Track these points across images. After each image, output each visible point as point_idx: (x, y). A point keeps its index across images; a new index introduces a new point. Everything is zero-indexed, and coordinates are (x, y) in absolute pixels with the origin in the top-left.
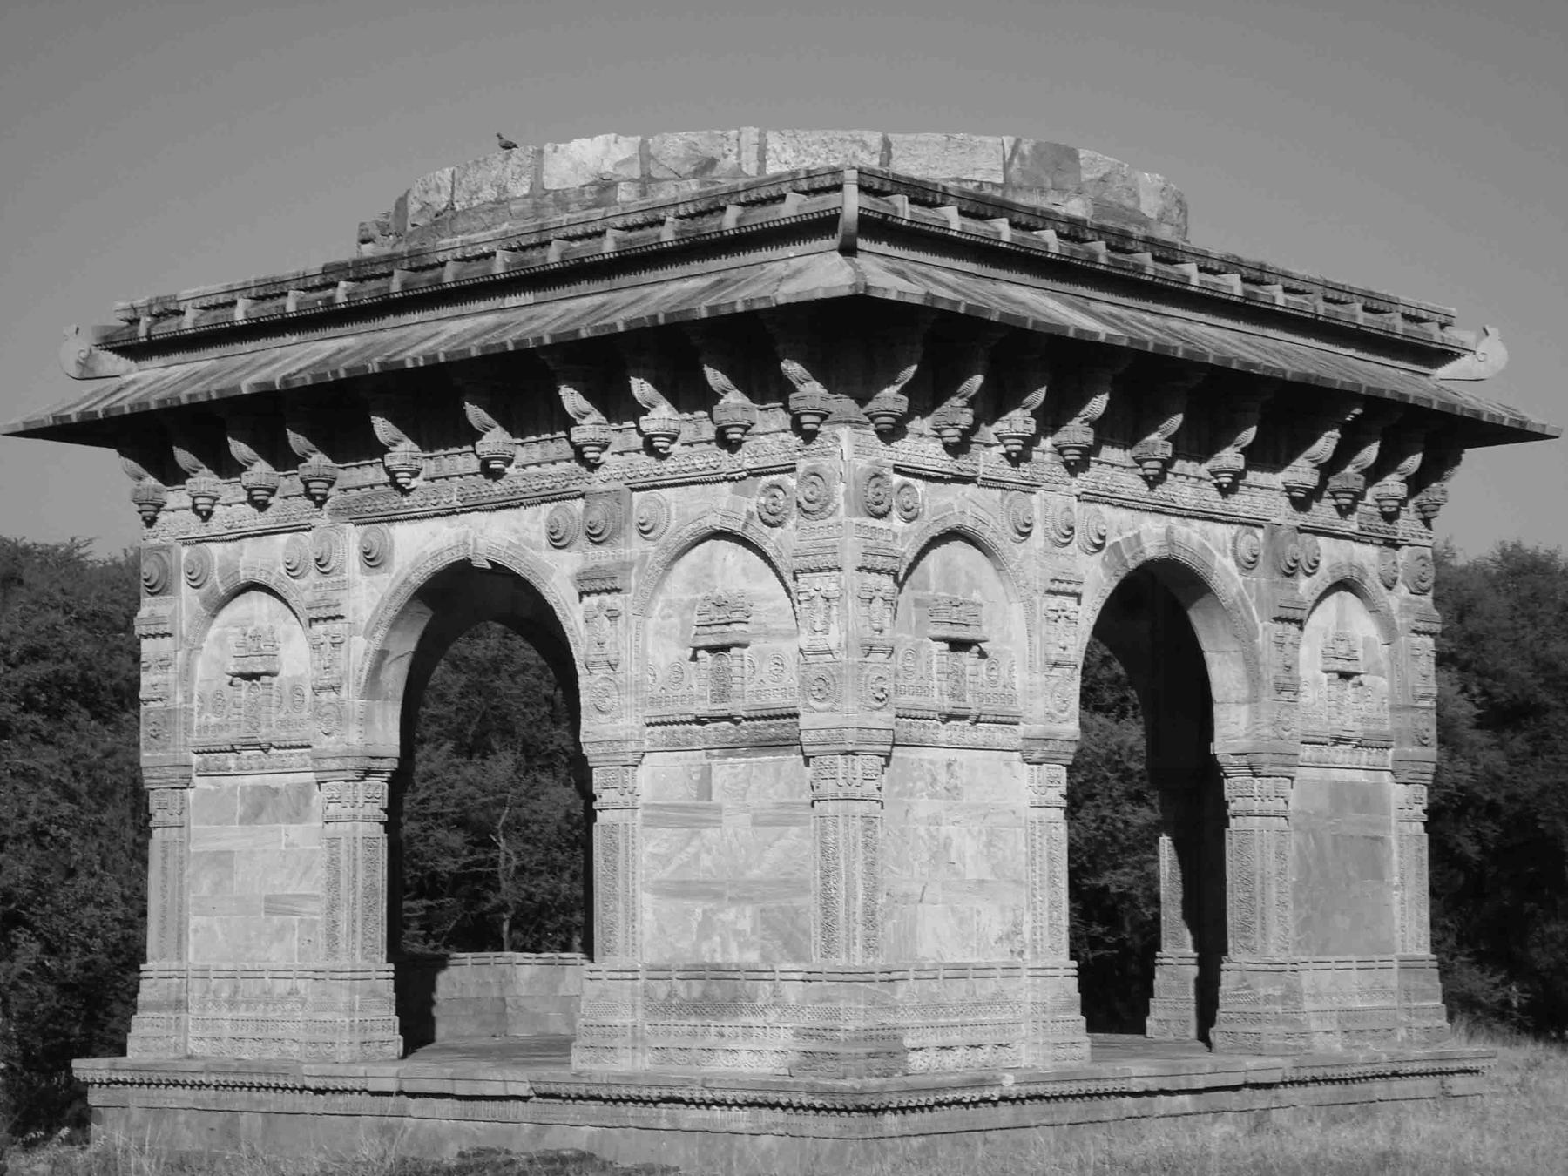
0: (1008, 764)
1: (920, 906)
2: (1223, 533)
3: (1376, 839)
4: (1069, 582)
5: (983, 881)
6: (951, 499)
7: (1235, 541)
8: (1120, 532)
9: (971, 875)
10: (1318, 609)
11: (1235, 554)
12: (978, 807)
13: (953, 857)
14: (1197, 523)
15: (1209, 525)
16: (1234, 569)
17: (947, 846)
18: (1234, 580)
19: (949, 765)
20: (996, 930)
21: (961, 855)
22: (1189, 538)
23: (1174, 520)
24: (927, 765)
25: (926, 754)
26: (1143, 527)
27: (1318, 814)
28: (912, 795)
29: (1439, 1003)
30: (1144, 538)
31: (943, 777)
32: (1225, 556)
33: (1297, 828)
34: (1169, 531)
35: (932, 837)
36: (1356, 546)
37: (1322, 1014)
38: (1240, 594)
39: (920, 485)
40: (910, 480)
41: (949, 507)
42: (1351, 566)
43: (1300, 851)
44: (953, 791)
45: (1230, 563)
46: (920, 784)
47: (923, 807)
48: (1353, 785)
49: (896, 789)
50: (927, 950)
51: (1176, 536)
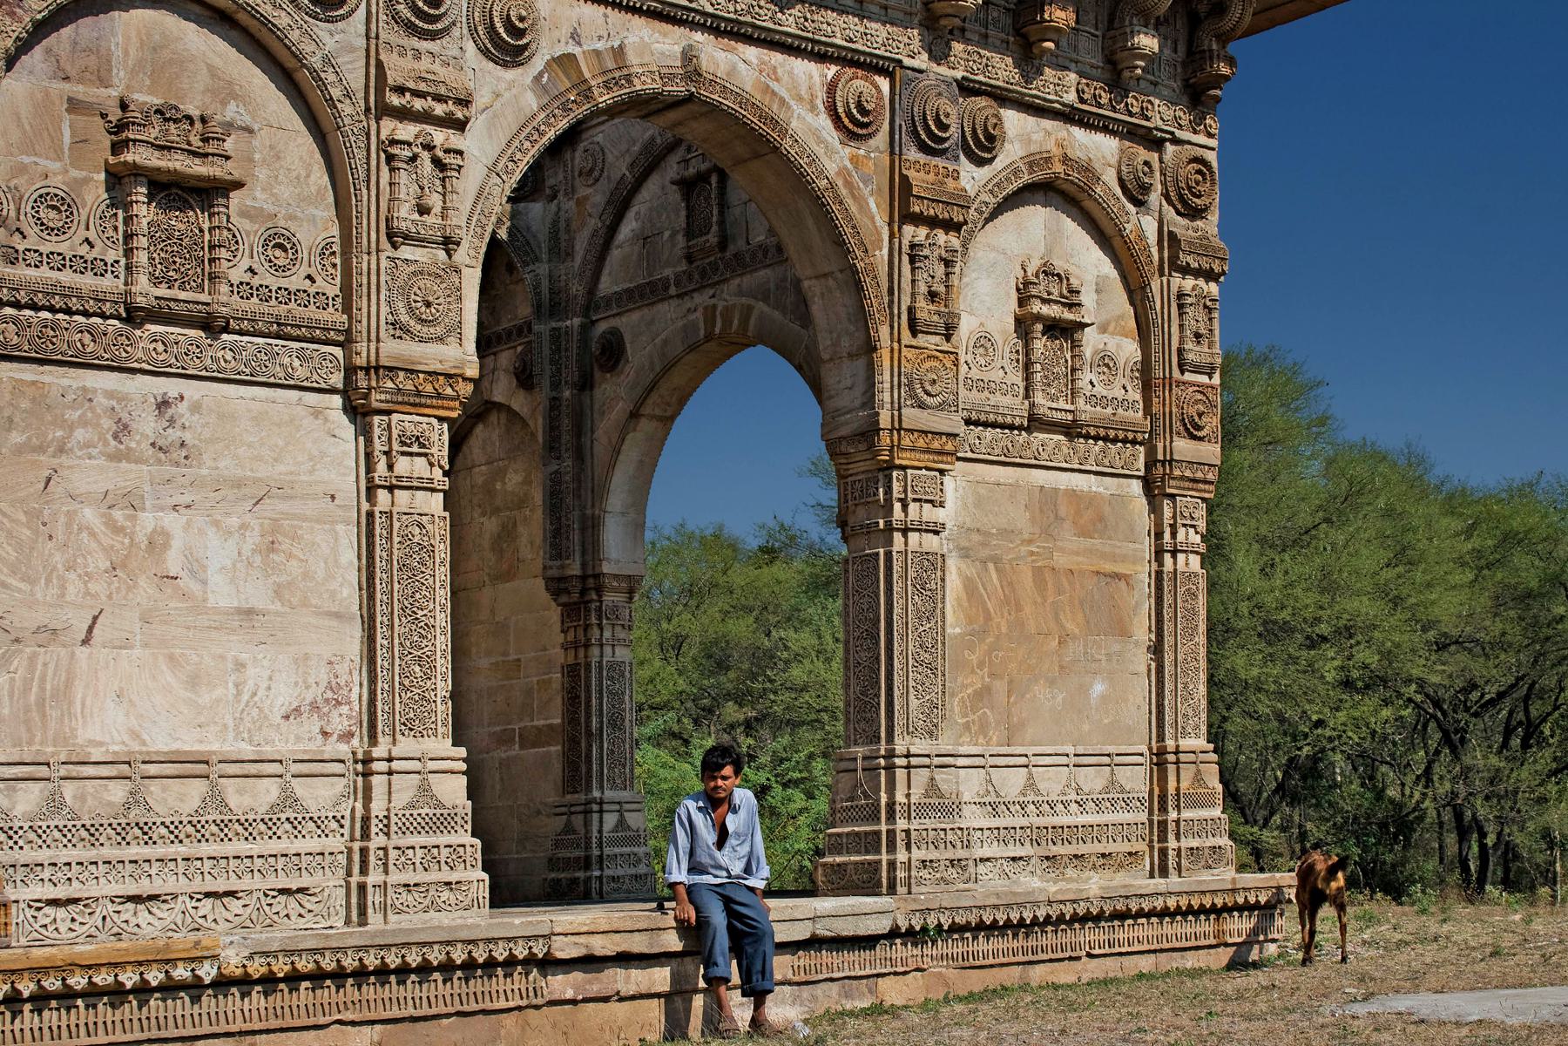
0: (317, 413)
1: (82, 653)
2: (809, 74)
3: (1117, 576)
4: (439, 98)
5: (249, 612)
7: (832, 88)
8: (575, 37)
9: (222, 595)
10: (1008, 218)
11: (832, 110)
12: (238, 484)
13: (173, 564)
14: (752, 53)
15: (777, 58)
17: (157, 543)
18: (830, 151)
20: (284, 696)
21: (196, 568)
22: (733, 70)
23: (698, 36)
24: (101, 401)
26: (631, 40)
27: (1005, 533)
28: (61, 450)
29: (1217, 812)
30: (632, 58)
31: (147, 425)
32: (813, 108)
33: (965, 553)
34: (688, 56)
35: (118, 530)
36: (1078, 133)
37: (1003, 835)
38: (842, 172)
42: (1066, 159)
43: (969, 586)
44: (183, 452)
45: (824, 122)
46: (80, 434)
47: (90, 474)
48: (1072, 494)
50: (104, 728)
51: (705, 65)
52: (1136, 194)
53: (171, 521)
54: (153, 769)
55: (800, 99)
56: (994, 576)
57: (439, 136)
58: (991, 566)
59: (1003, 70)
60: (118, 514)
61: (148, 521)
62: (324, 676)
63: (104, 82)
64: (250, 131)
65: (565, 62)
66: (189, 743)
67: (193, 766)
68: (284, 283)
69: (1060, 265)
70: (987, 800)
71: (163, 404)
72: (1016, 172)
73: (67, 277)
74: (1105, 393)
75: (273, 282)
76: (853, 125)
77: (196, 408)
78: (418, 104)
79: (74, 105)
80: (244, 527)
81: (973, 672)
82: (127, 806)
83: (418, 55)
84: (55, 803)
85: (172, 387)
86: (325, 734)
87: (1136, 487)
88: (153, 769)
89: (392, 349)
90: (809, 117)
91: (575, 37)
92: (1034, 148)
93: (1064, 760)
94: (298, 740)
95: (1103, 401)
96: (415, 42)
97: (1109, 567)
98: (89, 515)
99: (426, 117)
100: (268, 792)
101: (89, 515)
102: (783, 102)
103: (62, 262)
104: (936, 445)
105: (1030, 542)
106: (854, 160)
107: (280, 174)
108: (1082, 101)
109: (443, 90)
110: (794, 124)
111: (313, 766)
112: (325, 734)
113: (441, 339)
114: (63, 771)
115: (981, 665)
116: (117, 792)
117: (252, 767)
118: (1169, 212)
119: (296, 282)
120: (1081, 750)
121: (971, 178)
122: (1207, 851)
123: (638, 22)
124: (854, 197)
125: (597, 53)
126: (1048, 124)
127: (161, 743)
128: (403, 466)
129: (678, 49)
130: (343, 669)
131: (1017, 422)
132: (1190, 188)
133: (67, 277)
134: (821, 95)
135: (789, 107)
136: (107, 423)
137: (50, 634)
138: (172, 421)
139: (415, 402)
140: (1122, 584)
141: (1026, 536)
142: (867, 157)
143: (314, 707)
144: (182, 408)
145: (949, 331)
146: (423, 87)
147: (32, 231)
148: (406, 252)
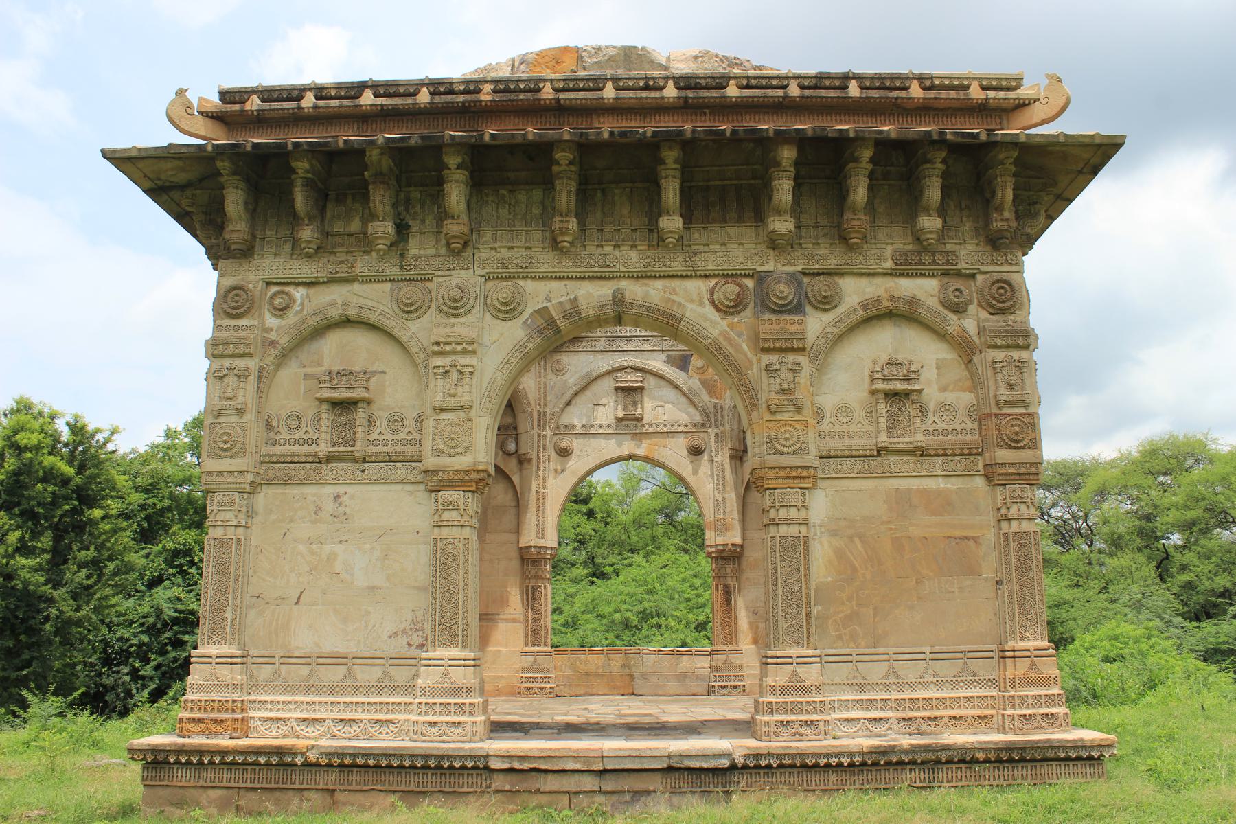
0: (411, 494)
5: (373, 588)
6: (333, 297)
8: (548, 299)
11: (713, 302)
14: (659, 284)
15: (676, 283)
16: (715, 316)
17: (331, 558)
19: (338, 496)
20: (389, 628)
23: (624, 283)
25: (309, 490)
28: (291, 521)
30: (582, 301)
31: (329, 506)
32: (701, 304)
35: (313, 553)
39: (298, 293)
40: (287, 289)
41: (333, 303)
42: (893, 298)
45: (709, 310)
49: (273, 517)
52: (958, 309)
53: (338, 548)
54: (321, 661)
55: (692, 301)
56: (859, 545)
57: (463, 360)
58: (857, 540)
59: (830, 258)
60: (314, 546)
61: (327, 548)
62: (410, 617)
63: (320, 365)
64: (384, 373)
65: (543, 312)
66: (340, 649)
67: (338, 659)
68: (395, 437)
69: (900, 357)
70: (854, 682)
71: (337, 497)
72: (854, 311)
73: (296, 448)
74: (946, 427)
75: (390, 437)
76: (729, 309)
77: (352, 497)
78: (448, 348)
79: (306, 377)
80: (372, 548)
81: (843, 603)
82: (310, 677)
83: (453, 325)
84: (276, 674)
85: (341, 489)
86: (409, 645)
87: (980, 482)
88: (321, 661)
89: (444, 461)
90: (699, 309)
91: (548, 299)
92: (867, 297)
93: (921, 656)
94: (398, 646)
95: (945, 433)
96: (452, 320)
97: (958, 533)
98: (301, 548)
99: (454, 352)
100: (377, 672)
101: (301, 548)
102: (680, 304)
103: (294, 442)
104: (794, 474)
105: (889, 522)
106: (731, 326)
107: (395, 390)
108: (897, 264)
109: (459, 339)
110: (688, 314)
111: (399, 661)
112: (409, 645)
113: (461, 454)
114: (282, 660)
115: (850, 599)
116: (305, 671)
117: (369, 660)
118: (984, 315)
119: (402, 435)
120: (937, 649)
121: (815, 324)
122: (1039, 718)
123: (586, 283)
124: (731, 344)
125: (561, 303)
126: (878, 281)
127: (328, 648)
128: (446, 516)
129: (610, 292)
130: (420, 614)
131: (868, 453)
132: (994, 299)
133: (296, 448)
134: (706, 296)
135: (684, 306)
136: (312, 508)
137: (280, 599)
138: (340, 504)
139: (451, 485)
140: (971, 543)
141: (885, 519)
142: (740, 322)
143: (404, 632)
144: (346, 497)
145: (798, 408)
146: (449, 340)
147: (284, 431)
148: (444, 416)
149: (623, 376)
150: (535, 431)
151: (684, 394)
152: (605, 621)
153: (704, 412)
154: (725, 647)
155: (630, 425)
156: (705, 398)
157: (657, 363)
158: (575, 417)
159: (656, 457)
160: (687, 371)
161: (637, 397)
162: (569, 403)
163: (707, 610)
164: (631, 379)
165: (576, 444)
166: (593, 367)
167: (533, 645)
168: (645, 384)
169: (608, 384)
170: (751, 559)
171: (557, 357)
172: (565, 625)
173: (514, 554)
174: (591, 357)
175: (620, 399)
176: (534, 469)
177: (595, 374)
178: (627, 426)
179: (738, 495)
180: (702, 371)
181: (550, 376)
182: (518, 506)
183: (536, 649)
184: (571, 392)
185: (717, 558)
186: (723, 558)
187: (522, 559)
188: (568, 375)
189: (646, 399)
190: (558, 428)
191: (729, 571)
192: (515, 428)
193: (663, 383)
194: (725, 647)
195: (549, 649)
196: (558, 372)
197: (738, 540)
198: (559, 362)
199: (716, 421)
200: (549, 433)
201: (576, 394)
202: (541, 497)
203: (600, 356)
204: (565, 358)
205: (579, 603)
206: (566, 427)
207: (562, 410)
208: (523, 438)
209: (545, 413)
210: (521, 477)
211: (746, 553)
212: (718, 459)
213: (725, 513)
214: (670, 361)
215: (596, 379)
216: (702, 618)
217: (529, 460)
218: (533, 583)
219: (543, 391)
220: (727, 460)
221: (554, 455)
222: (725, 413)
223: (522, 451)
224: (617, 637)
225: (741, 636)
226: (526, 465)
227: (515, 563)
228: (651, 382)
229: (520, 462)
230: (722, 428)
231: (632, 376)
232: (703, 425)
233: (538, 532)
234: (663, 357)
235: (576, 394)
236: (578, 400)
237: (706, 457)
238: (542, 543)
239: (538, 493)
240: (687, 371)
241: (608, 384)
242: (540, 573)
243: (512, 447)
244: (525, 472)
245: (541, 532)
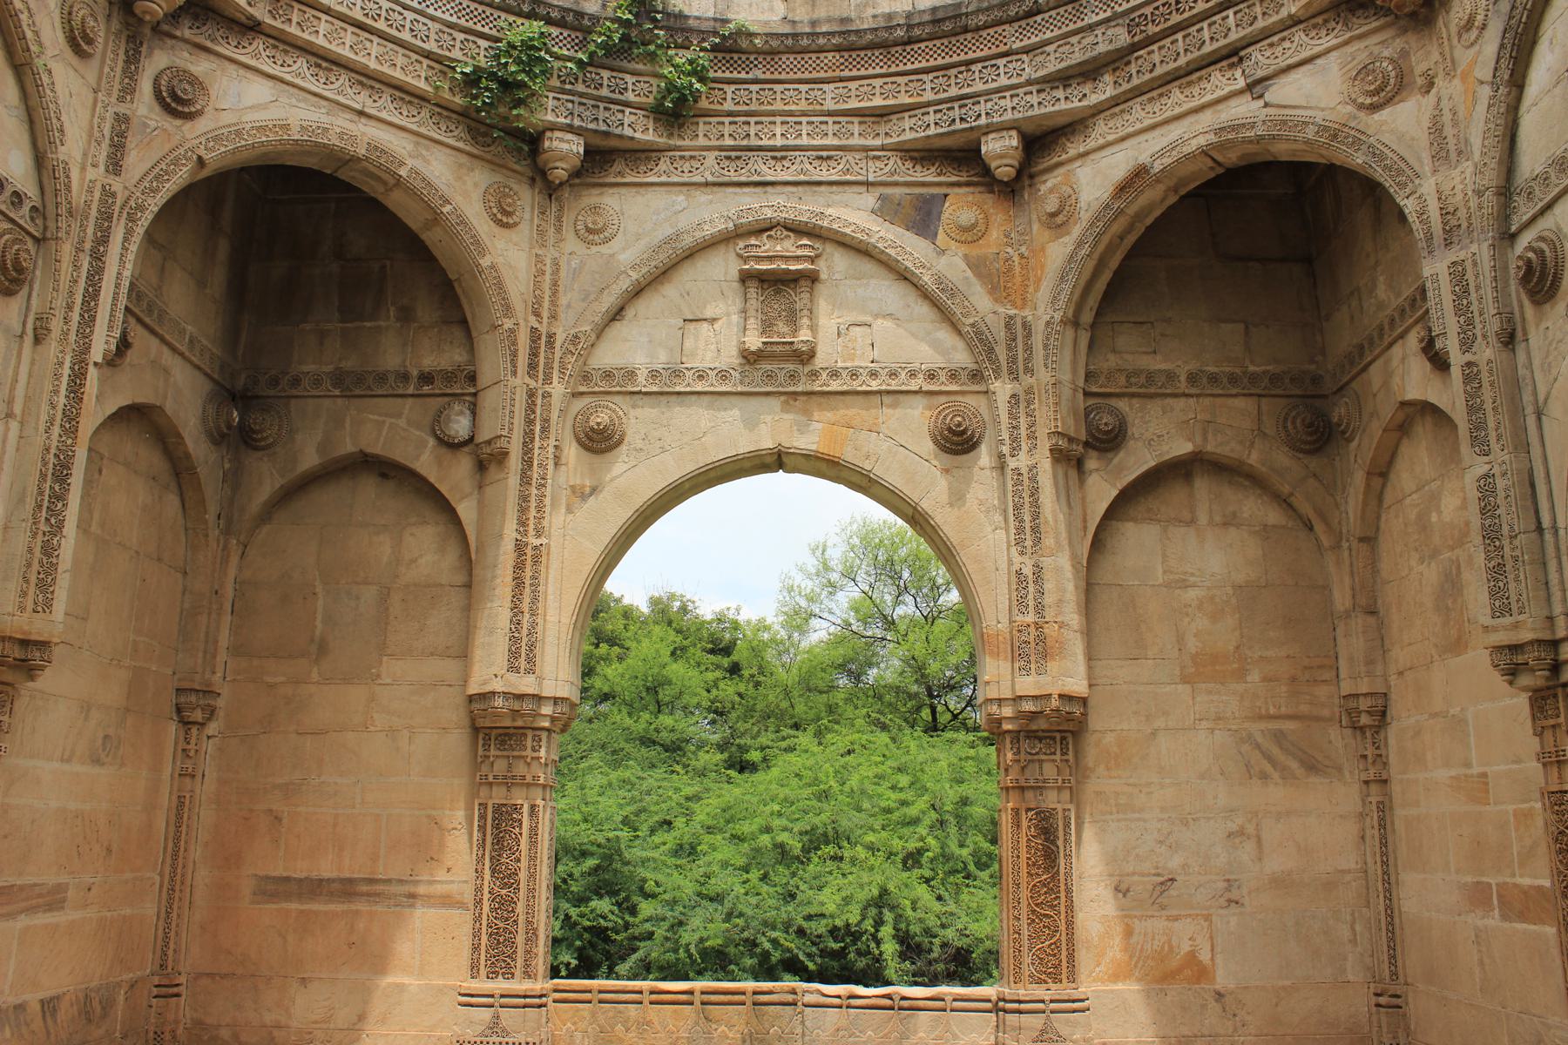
149: (766, 246)
150: (521, 381)
151: (925, 295)
152: (745, 847)
153: (979, 341)
154: (1039, 992)
155: (780, 369)
156: (981, 303)
157: (853, 213)
158: (636, 347)
159: (849, 455)
160: (932, 237)
161: (801, 299)
162: (617, 314)
163: (922, 830)
164: (784, 252)
165: (638, 421)
166: (684, 222)
167: (492, 975)
168: (821, 266)
169: (723, 267)
170: (1109, 739)
171: (591, 198)
172: (678, 851)
173: (454, 715)
174: (680, 199)
175: (754, 303)
176: (513, 481)
177: (688, 241)
178: (770, 376)
179: (1074, 557)
180: (970, 234)
181: (571, 244)
182: (468, 586)
183: (500, 985)
184: (625, 284)
185: (1016, 736)
186: (1032, 735)
187: (476, 730)
188: (615, 245)
189: (823, 306)
190: (586, 377)
191: (1049, 771)
192: (472, 378)
193: (867, 266)
194: (1039, 992)
195: (542, 984)
196: (594, 234)
197: (1078, 686)
198: (595, 209)
199: (1013, 360)
200: (558, 389)
201: (638, 292)
202: (527, 559)
203: (702, 197)
204: (611, 201)
205: (702, 814)
206: (608, 375)
207: (600, 332)
208: (489, 400)
209: (551, 337)
210: (481, 505)
211: (1096, 722)
212: (1022, 461)
213: (1040, 609)
214: (887, 210)
215: (691, 254)
216: (912, 845)
217: (502, 457)
218: (498, 796)
219: (548, 285)
220: (1046, 464)
221: (572, 452)
222: (1038, 340)
223: (482, 437)
224: (764, 878)
225: (1084, 958)
226: (493, 472)
227: (456, 742)
228: (835, 264)
229: (481, 466)
230: (1028, 380)
231: (788, 246)
232: (976, 376)
233: (514, 655)
234: (869, 199)
235: (638, 292)
236: (642, 306)
237: (984, 456)
238: (526, 684)
239: (520, 547)
240: (932, 237)
241: (723, 267)
242: (520, 769)
243: (460, 426)
244: (488, 490)
245: (522, 654)
